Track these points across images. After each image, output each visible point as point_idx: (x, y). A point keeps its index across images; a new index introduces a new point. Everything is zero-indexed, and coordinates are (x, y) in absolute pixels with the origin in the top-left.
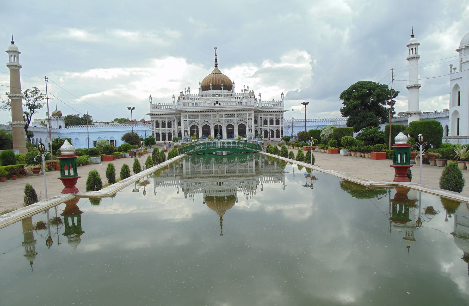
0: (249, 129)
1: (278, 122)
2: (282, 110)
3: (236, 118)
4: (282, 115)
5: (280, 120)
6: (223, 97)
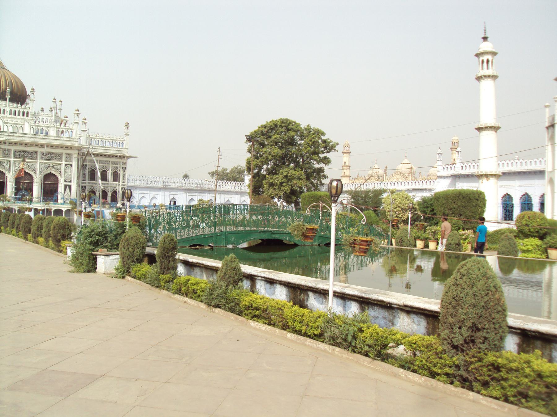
0: (66, 186)
1: (115, 177)
2: (126, 154)
3: (39, 161)
4: (125, 164)
5: (121, 172)
6: (7, 115)
